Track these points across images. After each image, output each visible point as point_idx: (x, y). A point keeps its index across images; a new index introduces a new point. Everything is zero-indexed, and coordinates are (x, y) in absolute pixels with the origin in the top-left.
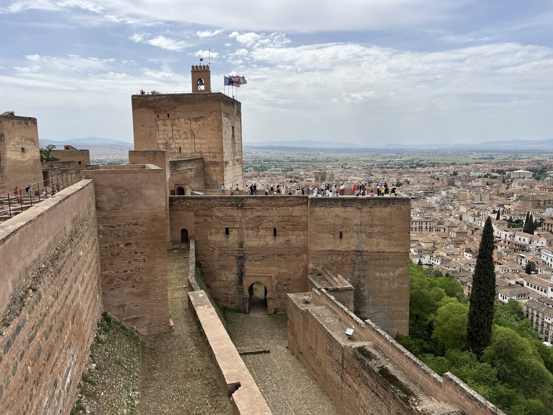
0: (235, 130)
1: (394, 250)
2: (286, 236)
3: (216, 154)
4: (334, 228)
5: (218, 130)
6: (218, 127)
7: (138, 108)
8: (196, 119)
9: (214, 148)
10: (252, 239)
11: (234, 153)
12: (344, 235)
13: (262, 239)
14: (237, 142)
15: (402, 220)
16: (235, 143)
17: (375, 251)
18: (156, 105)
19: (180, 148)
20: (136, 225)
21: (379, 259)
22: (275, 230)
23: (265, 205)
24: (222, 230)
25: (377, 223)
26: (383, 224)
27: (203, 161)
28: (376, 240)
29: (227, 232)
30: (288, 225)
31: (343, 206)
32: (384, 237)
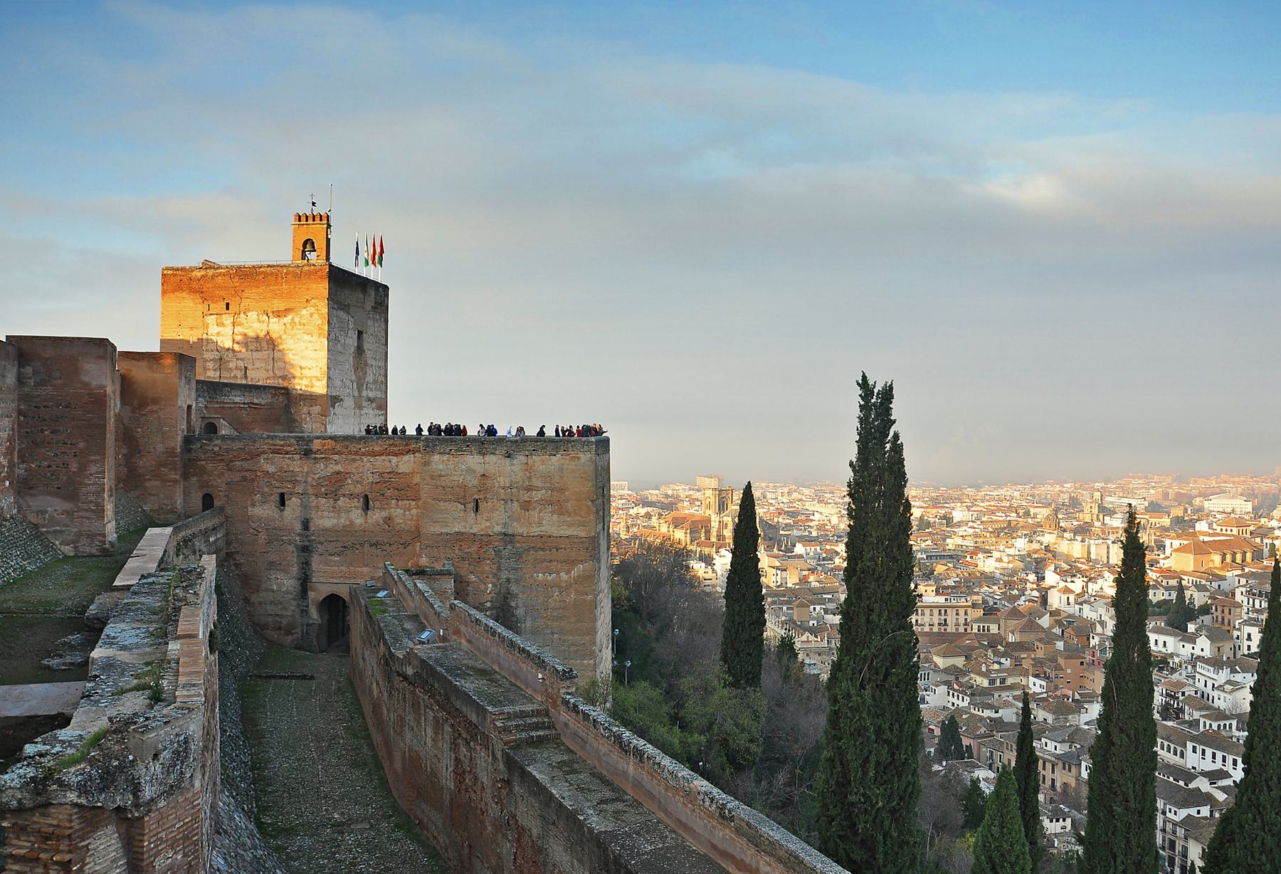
1: (568, 533)
2: (384, 509)
3: (314, 379)
4: (464, 492)
5: (320, 335)
6: (320, 328)
7: (173, 291)
8: (278, 314)
9: (309, 369)
12: (482, 505)
14: (371, 362)
16: (366, 365)
17: (536, 534)
19: (246, 368)
20: (67, 407)
21: (543, 549)
23: (350, 453)
25: (539, 484)
26: (549, 485)
27: (288, 394)
29: (282, 501)
32: (550, 508)
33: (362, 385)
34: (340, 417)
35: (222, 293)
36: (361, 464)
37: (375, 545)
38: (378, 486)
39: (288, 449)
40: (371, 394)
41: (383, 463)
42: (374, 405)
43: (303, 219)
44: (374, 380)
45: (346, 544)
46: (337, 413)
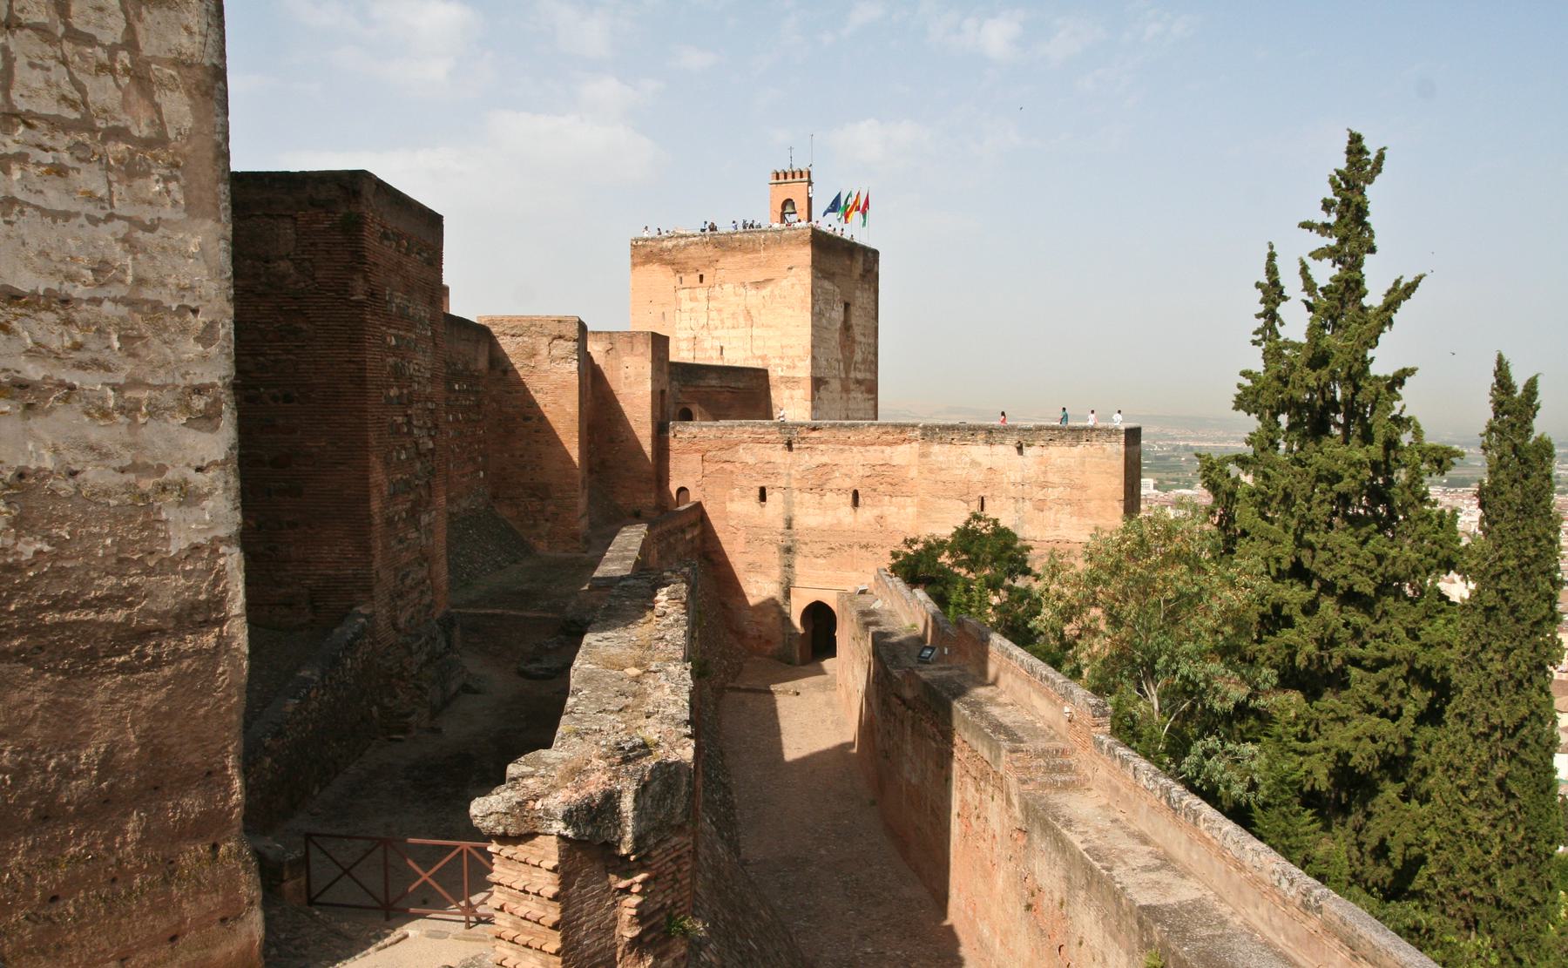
0: (856, 312)
5: (802, 308)
7: (644, 263)
8: (758, 285)
10: (811, 511)
11: (848, 363)
13: (829, 512)
14: (859, 338)
15: (1107, 473)
16: (854, 341)
18: (679, 256)
19: (722, 348)
22: (856, 494)
24: (752, 492)
26: (1068, 481)
28: (1052, 517)
30: (881, 484)
31: (987, 442)
33: (850, 366)
34: (826, 402)
35: (696, 264)
36: (851, 455)
37: (866, 547)
38: (868, 479)
39: (768, 437)
40: (860, 376)
41: (875, 454)
42: (863, 388)
43: (782, 176)
44: (863, 359)
45: (833, 546)
46: (822, 396)
